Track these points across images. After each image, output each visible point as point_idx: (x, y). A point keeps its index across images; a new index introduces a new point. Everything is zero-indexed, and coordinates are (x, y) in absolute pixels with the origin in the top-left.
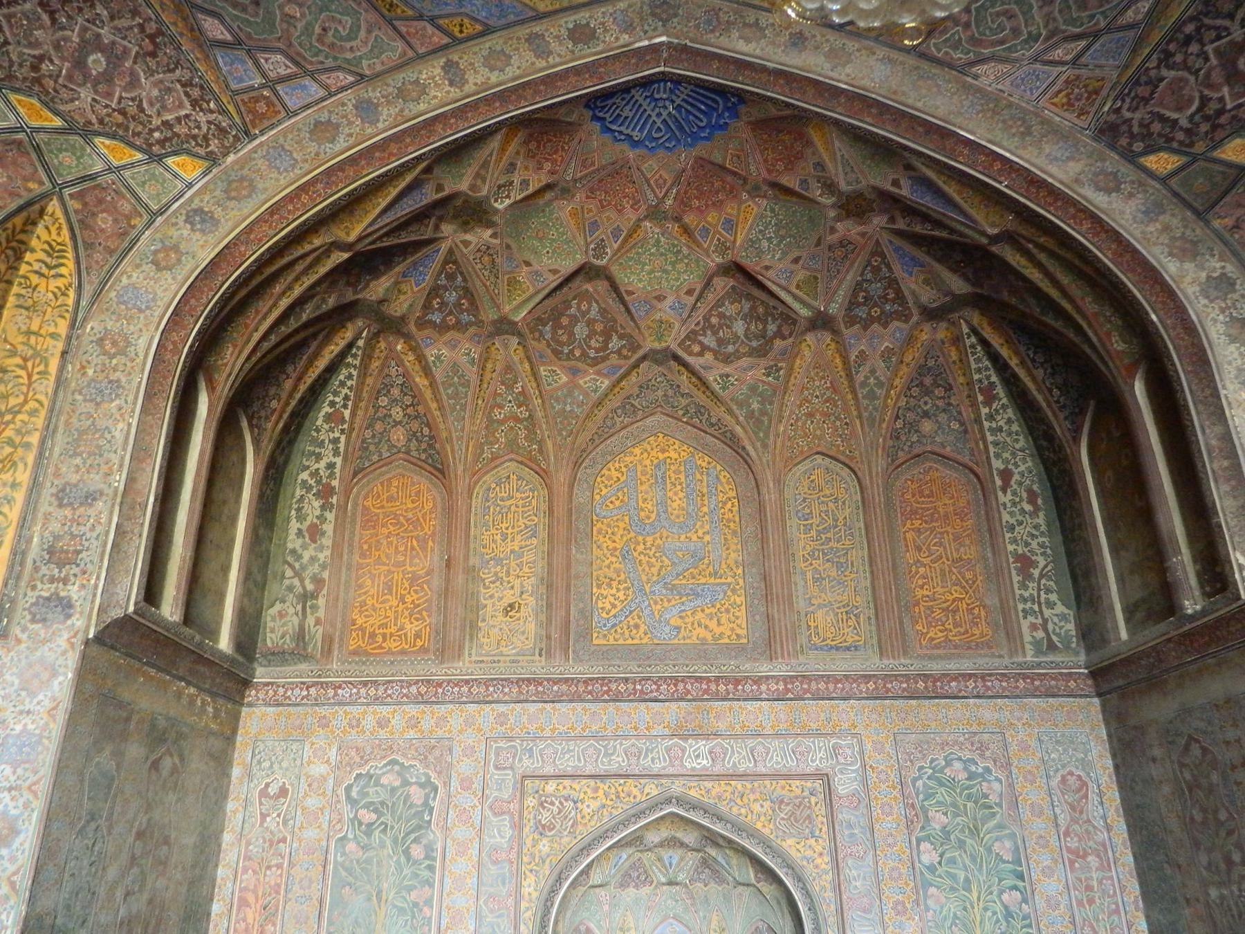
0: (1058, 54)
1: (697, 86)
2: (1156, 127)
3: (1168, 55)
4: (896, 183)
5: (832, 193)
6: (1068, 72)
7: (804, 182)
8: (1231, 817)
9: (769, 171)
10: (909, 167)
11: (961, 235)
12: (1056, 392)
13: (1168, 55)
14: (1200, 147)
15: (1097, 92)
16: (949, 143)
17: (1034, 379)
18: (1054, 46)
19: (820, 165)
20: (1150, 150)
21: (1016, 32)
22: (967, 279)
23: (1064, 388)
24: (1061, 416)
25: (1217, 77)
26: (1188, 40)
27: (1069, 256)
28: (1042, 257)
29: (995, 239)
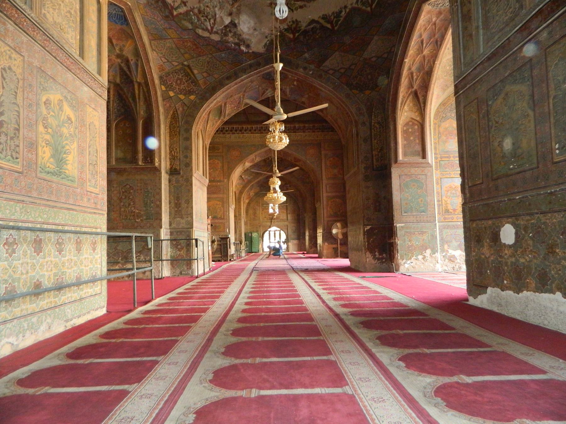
0: (163, 59)
1: (124, 16)
2: (165, 82)
3: (173, 73)
4: (132, 60)
5: (120, 51)
6: (162, 63)
7: (117, 45)
8: (133, 197)
9: (113, 36)
10: (137, 60)
11: (132, 76)
12: (116, 110)
13: (173, 73)
14: (168, 89)
15: (164, 70)
16: (147, 64)
17: (113, 105)
18: (163, 57)
19: (124, 46)
20: (163, 85)
21: (161, 50)
22: (121, 81)
23: (118, 110)
24: (114, 115)
25: (175, 80)
26: (176, 72)
27: (147, 94)
28: (141, 90)
29: (137, 82)
